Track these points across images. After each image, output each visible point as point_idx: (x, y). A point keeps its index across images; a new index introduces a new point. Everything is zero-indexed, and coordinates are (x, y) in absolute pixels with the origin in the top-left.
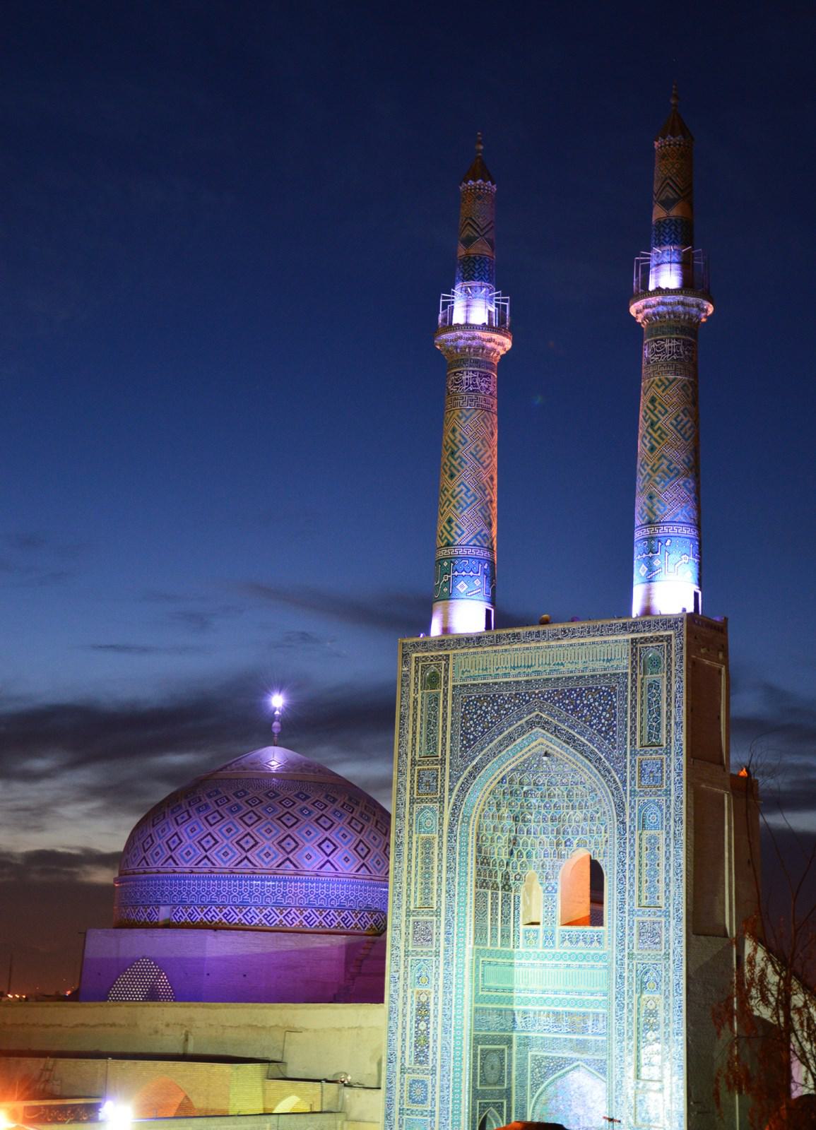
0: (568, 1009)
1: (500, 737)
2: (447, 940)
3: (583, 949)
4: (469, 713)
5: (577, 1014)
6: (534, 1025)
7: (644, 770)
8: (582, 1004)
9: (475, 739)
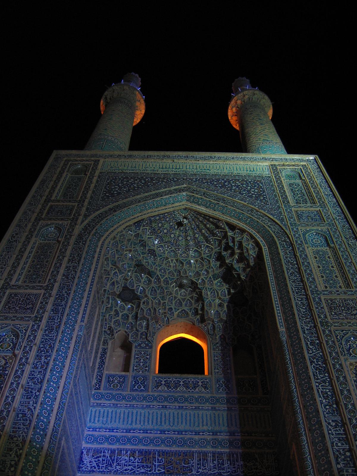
0: (163, 448)
1: (146, 194)
2: (55, 310)
3: (184, 392)
4: (114, 183)
5: (176, 453)
6: (111, 466)
7: (301, 215)
8: (183, 443)
9: (119, 194)
